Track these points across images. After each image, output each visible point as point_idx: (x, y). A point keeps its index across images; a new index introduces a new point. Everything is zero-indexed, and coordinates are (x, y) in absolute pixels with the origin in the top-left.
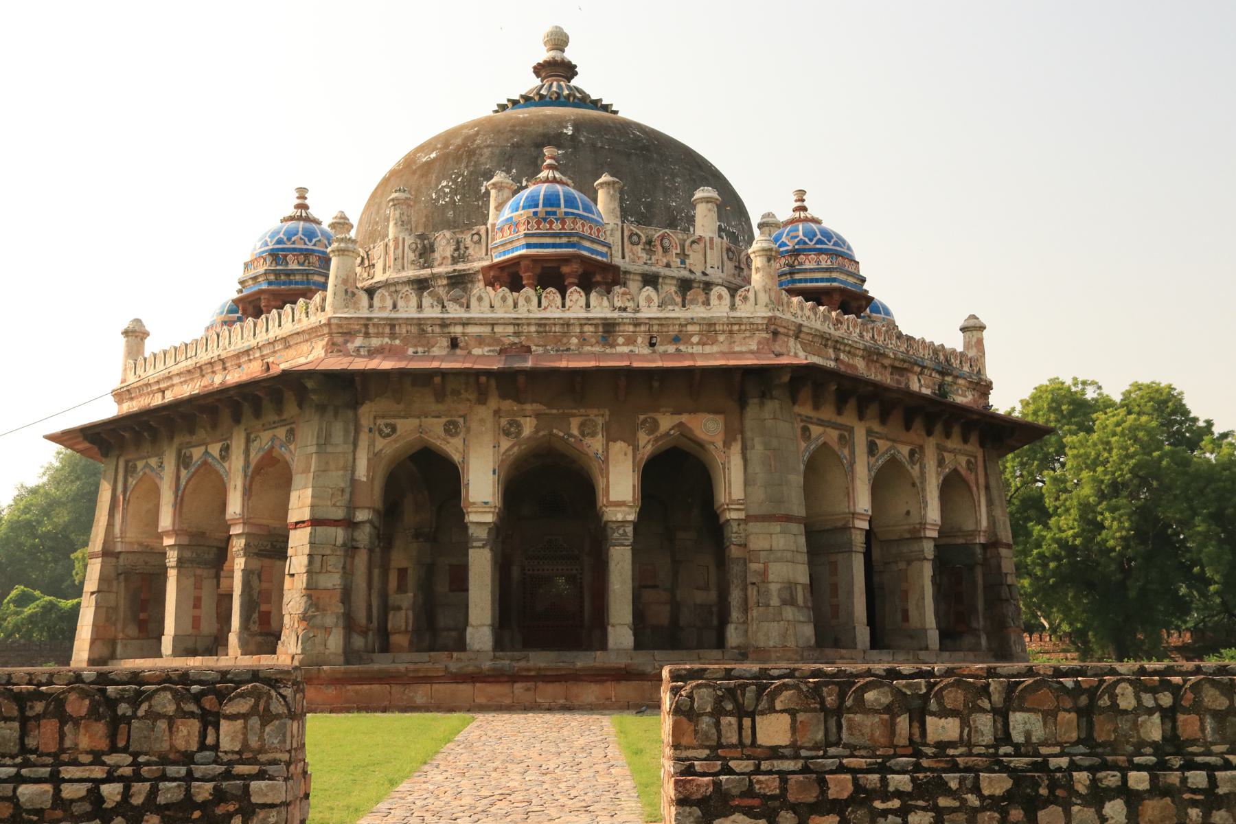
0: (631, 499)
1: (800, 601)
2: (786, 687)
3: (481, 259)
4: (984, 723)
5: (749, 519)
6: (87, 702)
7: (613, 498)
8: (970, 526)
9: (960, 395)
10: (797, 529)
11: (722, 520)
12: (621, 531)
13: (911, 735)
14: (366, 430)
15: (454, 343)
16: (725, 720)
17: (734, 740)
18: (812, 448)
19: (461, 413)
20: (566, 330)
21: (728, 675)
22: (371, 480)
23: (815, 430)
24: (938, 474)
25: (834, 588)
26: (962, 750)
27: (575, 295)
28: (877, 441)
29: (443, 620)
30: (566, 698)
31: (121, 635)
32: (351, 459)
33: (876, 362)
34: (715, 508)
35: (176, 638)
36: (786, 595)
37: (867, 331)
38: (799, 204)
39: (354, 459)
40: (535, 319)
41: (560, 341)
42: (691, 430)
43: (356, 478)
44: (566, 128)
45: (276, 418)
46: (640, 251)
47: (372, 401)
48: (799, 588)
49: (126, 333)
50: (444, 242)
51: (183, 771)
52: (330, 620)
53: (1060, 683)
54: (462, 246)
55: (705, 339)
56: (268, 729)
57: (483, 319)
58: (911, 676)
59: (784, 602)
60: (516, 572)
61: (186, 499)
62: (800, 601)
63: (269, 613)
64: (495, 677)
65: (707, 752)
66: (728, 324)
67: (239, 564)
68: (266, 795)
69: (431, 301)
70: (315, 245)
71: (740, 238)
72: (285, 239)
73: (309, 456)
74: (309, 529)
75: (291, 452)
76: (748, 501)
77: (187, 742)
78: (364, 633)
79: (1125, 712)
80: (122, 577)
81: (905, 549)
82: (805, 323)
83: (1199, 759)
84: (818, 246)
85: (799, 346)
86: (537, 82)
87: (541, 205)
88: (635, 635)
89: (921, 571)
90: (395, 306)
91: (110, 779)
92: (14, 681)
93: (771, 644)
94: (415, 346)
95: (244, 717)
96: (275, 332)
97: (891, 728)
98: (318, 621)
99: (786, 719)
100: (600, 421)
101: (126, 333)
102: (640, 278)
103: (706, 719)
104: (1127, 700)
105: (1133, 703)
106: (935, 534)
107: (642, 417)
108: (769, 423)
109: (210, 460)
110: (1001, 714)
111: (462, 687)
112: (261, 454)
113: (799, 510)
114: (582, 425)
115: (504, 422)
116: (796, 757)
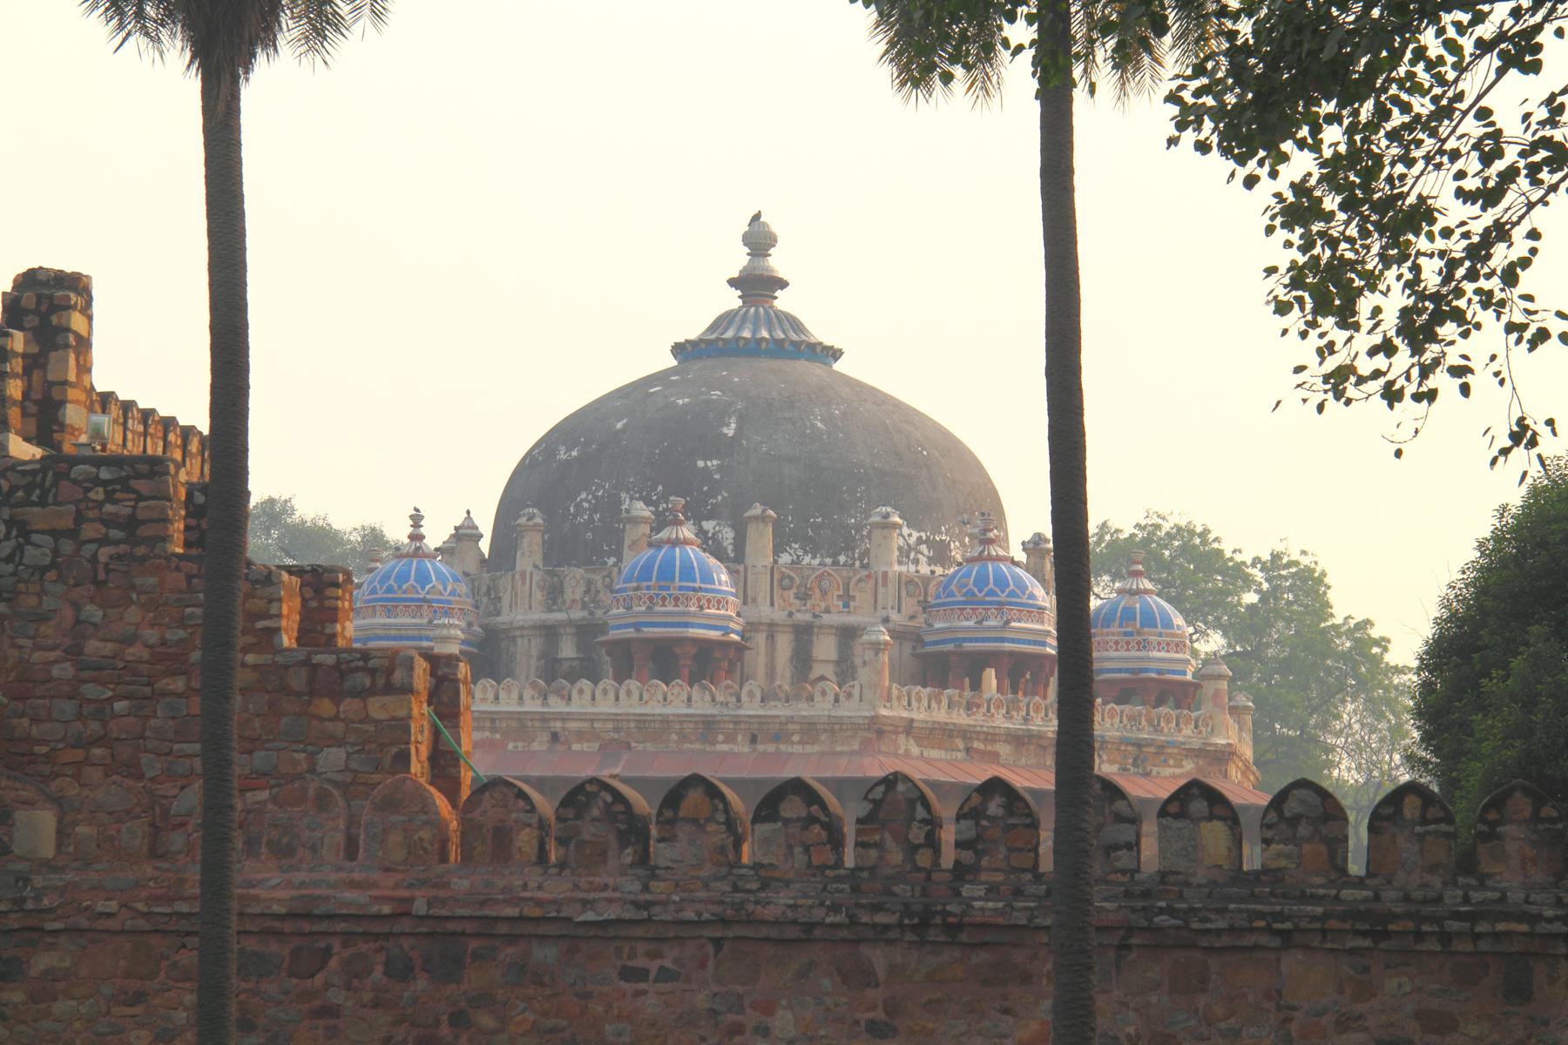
9: (1169, 766)
15: (555, 737)
27: (679, 689)
33: (1029, 743)
37: (1018, 709)
40: (635, 715)
44: (728, 425)
46: (792, 596)
50: (573, 582)
54: (593, 587)
66: (829, 724)
69: (532, 693)
70: (428, 593)
72: (395, 586)
84: (988, 599)
85: (912, 741)
86: (732, 300)
87: (654, 580)
90: (497, 698)
94: (515, 740)
102: (790, 629)
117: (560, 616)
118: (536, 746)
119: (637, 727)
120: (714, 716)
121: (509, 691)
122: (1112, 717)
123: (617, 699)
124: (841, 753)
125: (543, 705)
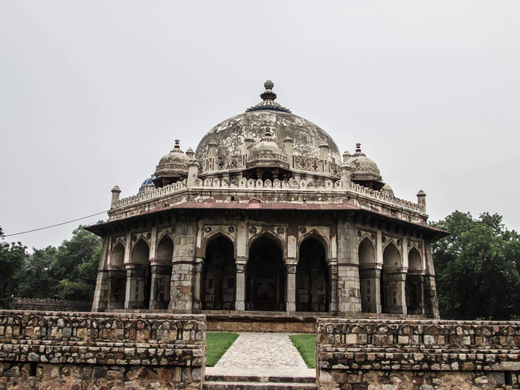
0: (295, 256)
1: (357, 295)
2: (355, 326)
3: (241, 167)
4: (416, 338)
5: (337, 265)
6: (144, 324)
7: (289, 256)
8: (419, 269)
10: (356, 269)
11: (328, 265)
12: (292, 268)
13: (394, 341)
14: (201, 229)
15: (233, 199)
16: (336, 336)
17: (339, 341)
18: (362, 239)
19: (235, 224)
20: (273, 195)
21: (337, 322)
22: (202, 248)
23: (363, 233)
24: (408, 249)
25: (369, 290)
26: (410, 346)
27: (277, 182)
28: (386, 237)
29: (226, 298)
30: (271, 329)
31: (109, 300)
32: (195, 239)
33: (386, 208)
34: (326, 260)
35: (130, 302)
36: (351, 293)
37: (382, 197)
38: (358, 149)
39: (196, 240)
41: (271, 199)
42: (318, 232)
43: (197, 246)
45: (168, 224)
47: (203, 219)
48: (356, 290)
49: (113, 191)
51: (173, 345)
52: (187, 298)
53: (440, 326)
54: (235, 162)
55: (323, 199)
56: (197, 334)
57: (243, 190)
58: (394, 324)
59: (351, 296)
60: (252, 282)
61: (134, 252)
62: (357, 295)
63: (163, 294)
64: (246, 320)
65: (331, 345)
66: (332, 194)
67: (154, 276)
68: (197, 354)
71: (336, 160)
73: (180, 239)
74: (181, 265)
75: (173, 236)
76: (338, 258)
77: (173, 337)
78: (198, 303)
79: (460, 336)
80: (110, 280)
81: (395, 277)
82: (360, 194)
83: (481, 350)
85: (357, 202)
88: (296, 306)
89: (401, 284)
90: (212, 185)
91: (151, 347)
92: (122, 317)
93: (346, 311)
94: (219, 199)
95: (191, 330)
96: (168, 193)
97: (386, 339)
98: (183, 298)
99: (355, 335)
100: (285, 228)
101: (113, 191)
103: (331, 335)
104: (460, 332)
105: (462, 333)
106: (406, 271)
107: (300, 227)
108: (346, 230)
109: (143, 238)
110: (422, 336)
111: (234, 323)
112: (162, 237)
113: (357, 262)
114: (278, 230)
115: (250, 227)
116: (359, 347)
117: (225, 170)
118: (226, 201)
119: (263, 195)
120: (291, 191)
121: (216, 182)
122: (403, 203)
123: (255, 185)
124: (337, 204)
125: (229, 187)
